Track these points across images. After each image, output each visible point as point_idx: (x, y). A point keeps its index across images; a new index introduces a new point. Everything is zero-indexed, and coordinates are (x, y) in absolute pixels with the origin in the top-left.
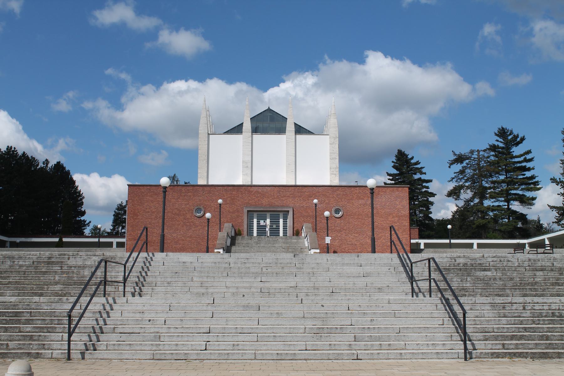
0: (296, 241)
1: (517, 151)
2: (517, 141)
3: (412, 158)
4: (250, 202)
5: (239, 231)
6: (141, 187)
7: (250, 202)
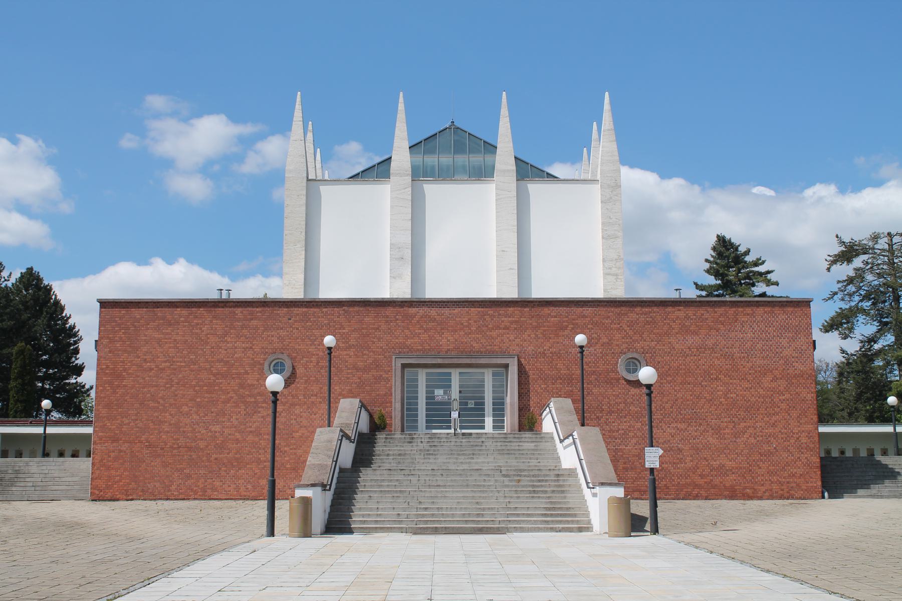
3: (747, 252)
4: (409, 342)
5: (382, 417)
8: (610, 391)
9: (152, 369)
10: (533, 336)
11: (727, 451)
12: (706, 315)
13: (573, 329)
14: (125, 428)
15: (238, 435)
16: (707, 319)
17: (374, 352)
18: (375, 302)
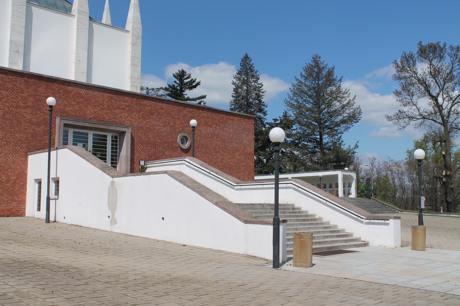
1: (189, 93)
2: (193, 85)
4: (67, 109)
7: (67, 109)
10: (137, 116)
13: (157, 115)
17: (44, 113)
18: (46, 78)
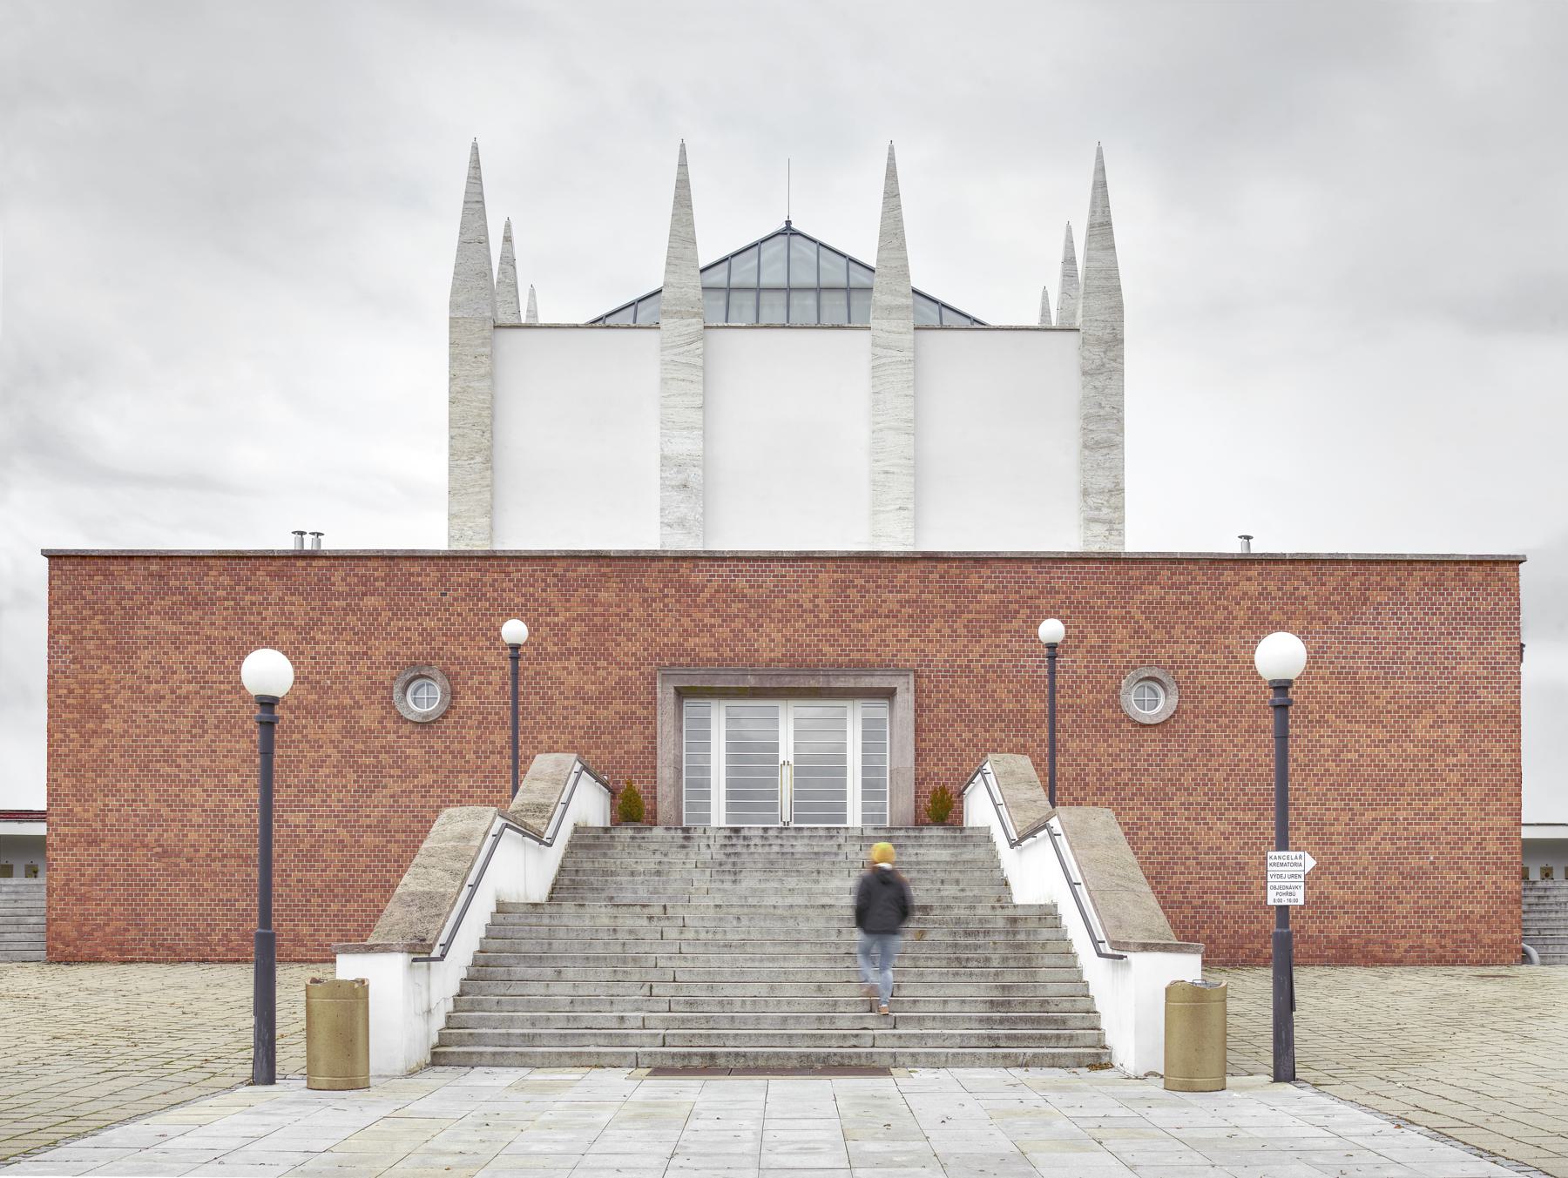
0: (945, 855)
6: (115, 567)
7: (692, 642)
8: (1102, 747)
9: (163, 697)
10: (947, 631)
11: (1335, 869)
12: (1304, 590)
14: (111, 818)
15: (342, 833)
16: (1305, 598)
